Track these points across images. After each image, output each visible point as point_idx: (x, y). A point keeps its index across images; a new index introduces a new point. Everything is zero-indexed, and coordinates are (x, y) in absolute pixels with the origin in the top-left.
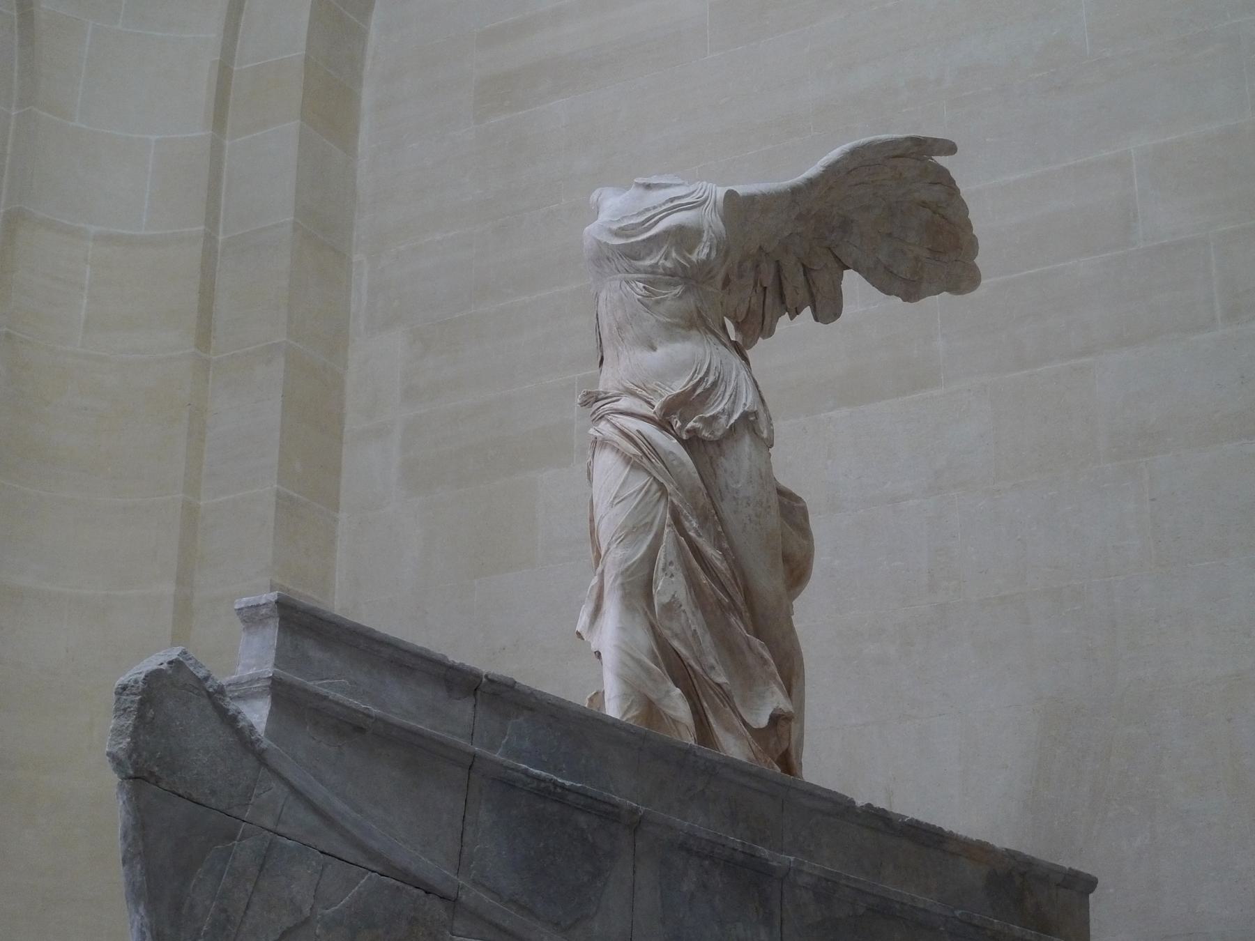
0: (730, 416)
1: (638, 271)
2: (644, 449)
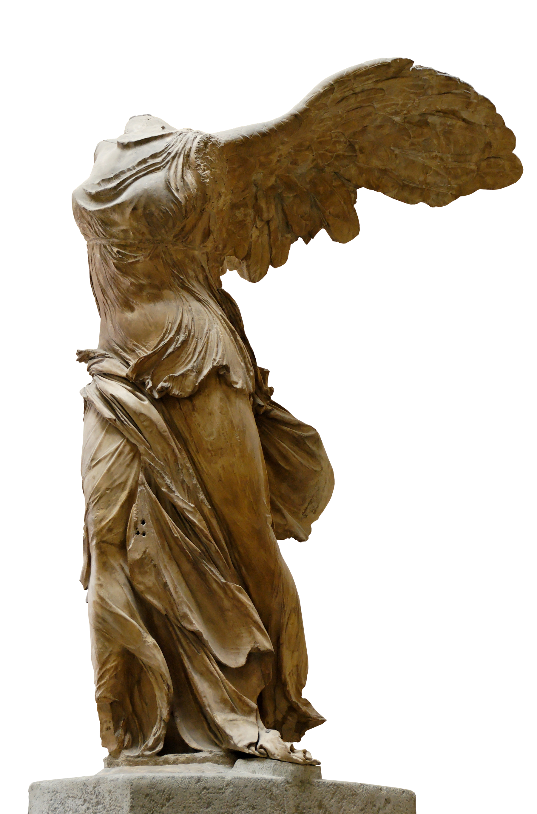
0: (199, 372)
1: (112, 236)
2: (118, 412)
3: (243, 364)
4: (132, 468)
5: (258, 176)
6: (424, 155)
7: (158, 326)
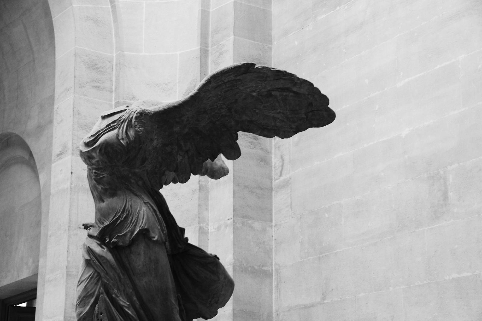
0: (132, 233)
1: (93, 164)
3: (159, 227)
4: (98, 285)
5: (177, 129)
6: (273, 112)
7: (113, 209)
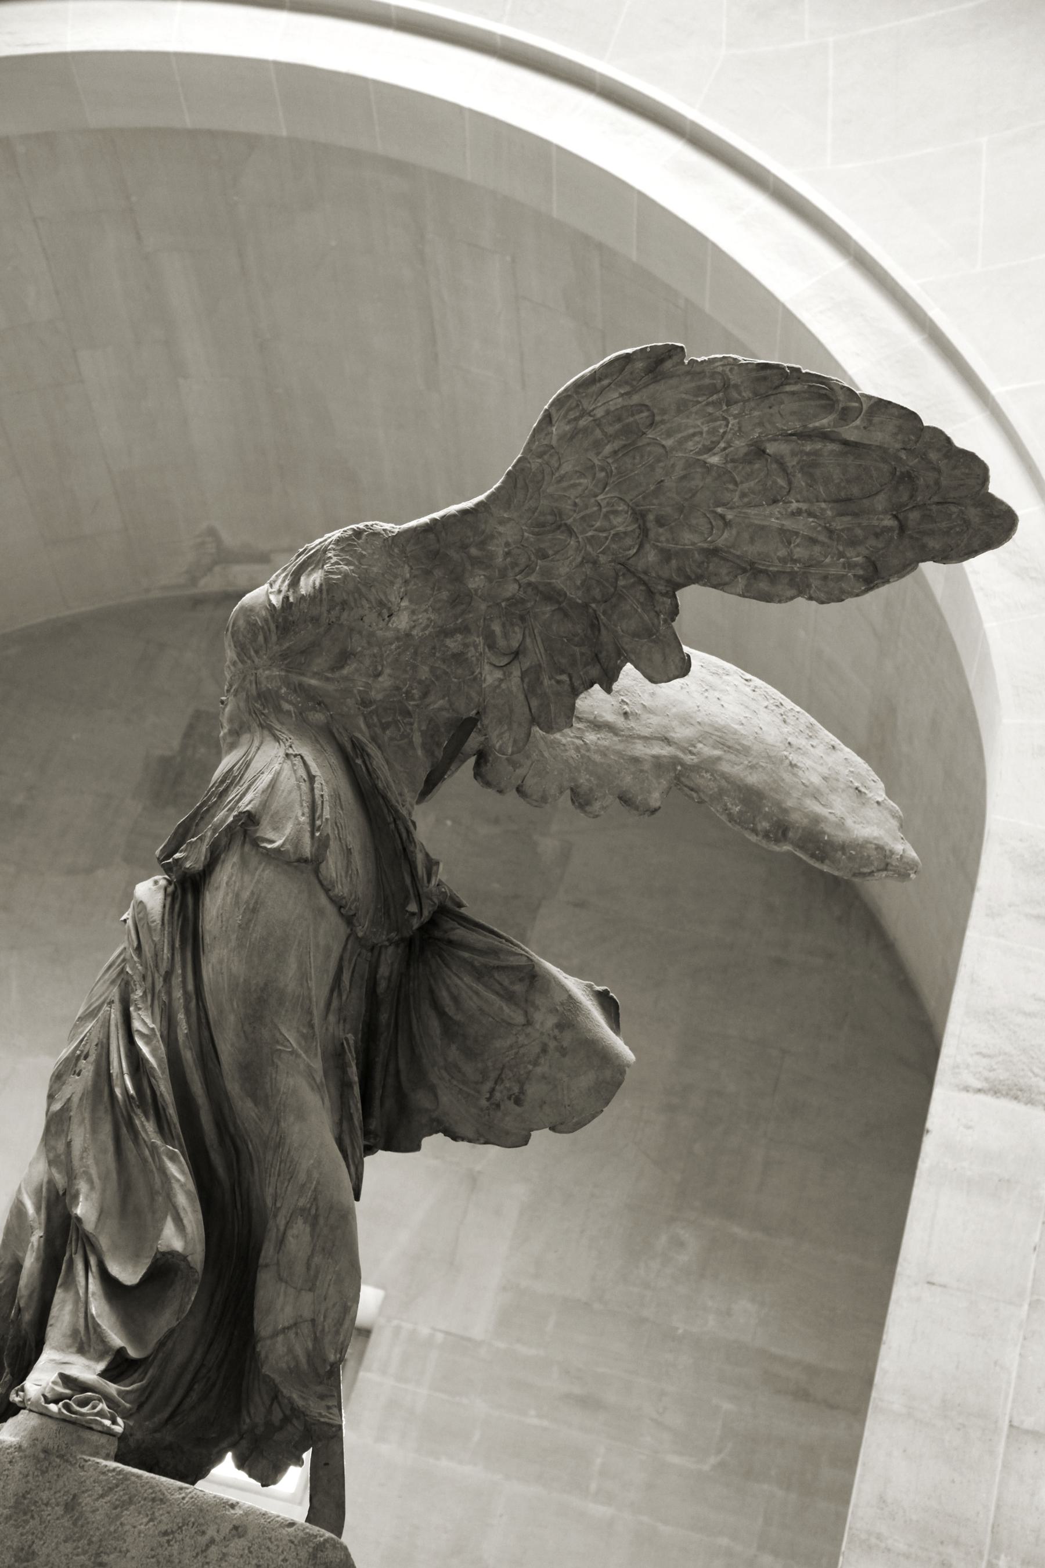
5: (476, 581)
